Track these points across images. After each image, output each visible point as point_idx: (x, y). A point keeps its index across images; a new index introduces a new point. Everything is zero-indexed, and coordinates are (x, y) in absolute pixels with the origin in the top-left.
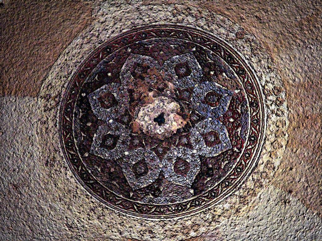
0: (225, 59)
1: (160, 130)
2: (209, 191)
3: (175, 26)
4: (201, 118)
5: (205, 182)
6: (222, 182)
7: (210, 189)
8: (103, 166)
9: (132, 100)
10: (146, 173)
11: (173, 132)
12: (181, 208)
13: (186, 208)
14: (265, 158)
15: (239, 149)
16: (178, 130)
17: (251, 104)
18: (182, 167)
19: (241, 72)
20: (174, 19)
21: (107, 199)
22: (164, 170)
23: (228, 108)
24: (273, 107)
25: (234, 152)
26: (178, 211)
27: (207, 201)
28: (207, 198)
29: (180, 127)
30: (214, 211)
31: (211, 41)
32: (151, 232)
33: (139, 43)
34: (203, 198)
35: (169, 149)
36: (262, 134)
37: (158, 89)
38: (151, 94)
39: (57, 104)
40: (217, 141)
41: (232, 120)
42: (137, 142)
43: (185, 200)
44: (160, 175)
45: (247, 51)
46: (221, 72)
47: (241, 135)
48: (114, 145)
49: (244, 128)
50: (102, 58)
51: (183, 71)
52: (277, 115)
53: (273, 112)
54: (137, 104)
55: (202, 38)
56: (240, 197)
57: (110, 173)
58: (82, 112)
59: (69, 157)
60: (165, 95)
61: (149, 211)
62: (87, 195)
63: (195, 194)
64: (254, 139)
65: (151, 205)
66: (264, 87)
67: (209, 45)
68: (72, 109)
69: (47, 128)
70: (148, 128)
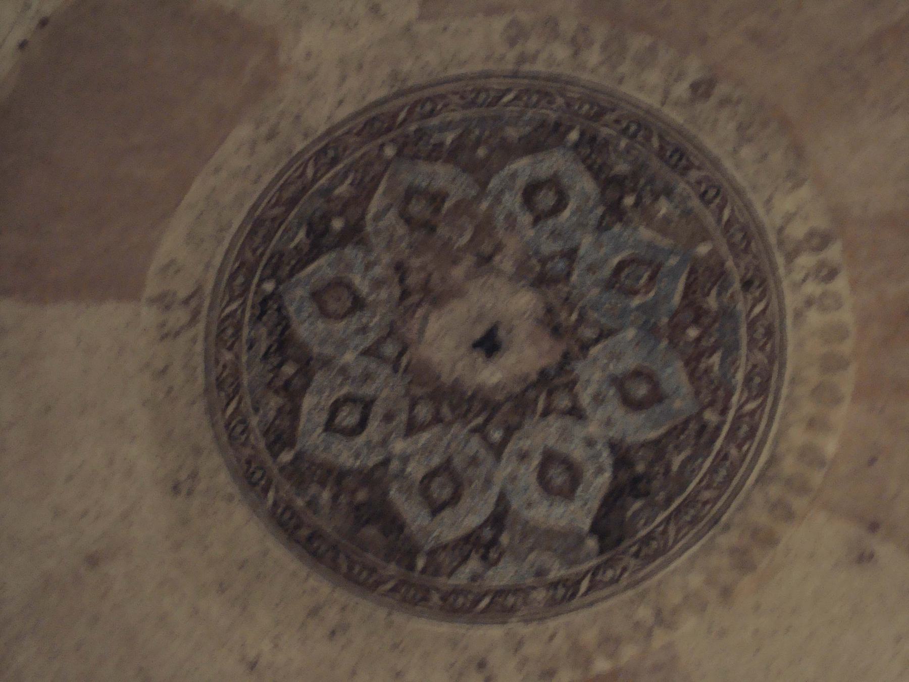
1: (491, 375)
3: (515, 75)
7: (643, 533)
10: (455, 499)
12: (565, 594)
14: (798, 436)
16: (543, 374)
17: (747, 285)
19: (715, 192)
20: (512, 55)
22: (510, 487)
24: (812, 288)
29: (544, 362)
36: (783, 366)
38: (458, 272)
40: (657, 397)
42: (423, 412)
45: (728, 129)
48: (362, 424)
49: (731, 350)
50: (315, 180)
51: (546, 199)
52: (824, 309)
53: (809, 302)
54: (419, 304)
56: (733, 551)
63: (602, 551)
64: (762, 384)
66: (781, 230)
68: (238, 329)
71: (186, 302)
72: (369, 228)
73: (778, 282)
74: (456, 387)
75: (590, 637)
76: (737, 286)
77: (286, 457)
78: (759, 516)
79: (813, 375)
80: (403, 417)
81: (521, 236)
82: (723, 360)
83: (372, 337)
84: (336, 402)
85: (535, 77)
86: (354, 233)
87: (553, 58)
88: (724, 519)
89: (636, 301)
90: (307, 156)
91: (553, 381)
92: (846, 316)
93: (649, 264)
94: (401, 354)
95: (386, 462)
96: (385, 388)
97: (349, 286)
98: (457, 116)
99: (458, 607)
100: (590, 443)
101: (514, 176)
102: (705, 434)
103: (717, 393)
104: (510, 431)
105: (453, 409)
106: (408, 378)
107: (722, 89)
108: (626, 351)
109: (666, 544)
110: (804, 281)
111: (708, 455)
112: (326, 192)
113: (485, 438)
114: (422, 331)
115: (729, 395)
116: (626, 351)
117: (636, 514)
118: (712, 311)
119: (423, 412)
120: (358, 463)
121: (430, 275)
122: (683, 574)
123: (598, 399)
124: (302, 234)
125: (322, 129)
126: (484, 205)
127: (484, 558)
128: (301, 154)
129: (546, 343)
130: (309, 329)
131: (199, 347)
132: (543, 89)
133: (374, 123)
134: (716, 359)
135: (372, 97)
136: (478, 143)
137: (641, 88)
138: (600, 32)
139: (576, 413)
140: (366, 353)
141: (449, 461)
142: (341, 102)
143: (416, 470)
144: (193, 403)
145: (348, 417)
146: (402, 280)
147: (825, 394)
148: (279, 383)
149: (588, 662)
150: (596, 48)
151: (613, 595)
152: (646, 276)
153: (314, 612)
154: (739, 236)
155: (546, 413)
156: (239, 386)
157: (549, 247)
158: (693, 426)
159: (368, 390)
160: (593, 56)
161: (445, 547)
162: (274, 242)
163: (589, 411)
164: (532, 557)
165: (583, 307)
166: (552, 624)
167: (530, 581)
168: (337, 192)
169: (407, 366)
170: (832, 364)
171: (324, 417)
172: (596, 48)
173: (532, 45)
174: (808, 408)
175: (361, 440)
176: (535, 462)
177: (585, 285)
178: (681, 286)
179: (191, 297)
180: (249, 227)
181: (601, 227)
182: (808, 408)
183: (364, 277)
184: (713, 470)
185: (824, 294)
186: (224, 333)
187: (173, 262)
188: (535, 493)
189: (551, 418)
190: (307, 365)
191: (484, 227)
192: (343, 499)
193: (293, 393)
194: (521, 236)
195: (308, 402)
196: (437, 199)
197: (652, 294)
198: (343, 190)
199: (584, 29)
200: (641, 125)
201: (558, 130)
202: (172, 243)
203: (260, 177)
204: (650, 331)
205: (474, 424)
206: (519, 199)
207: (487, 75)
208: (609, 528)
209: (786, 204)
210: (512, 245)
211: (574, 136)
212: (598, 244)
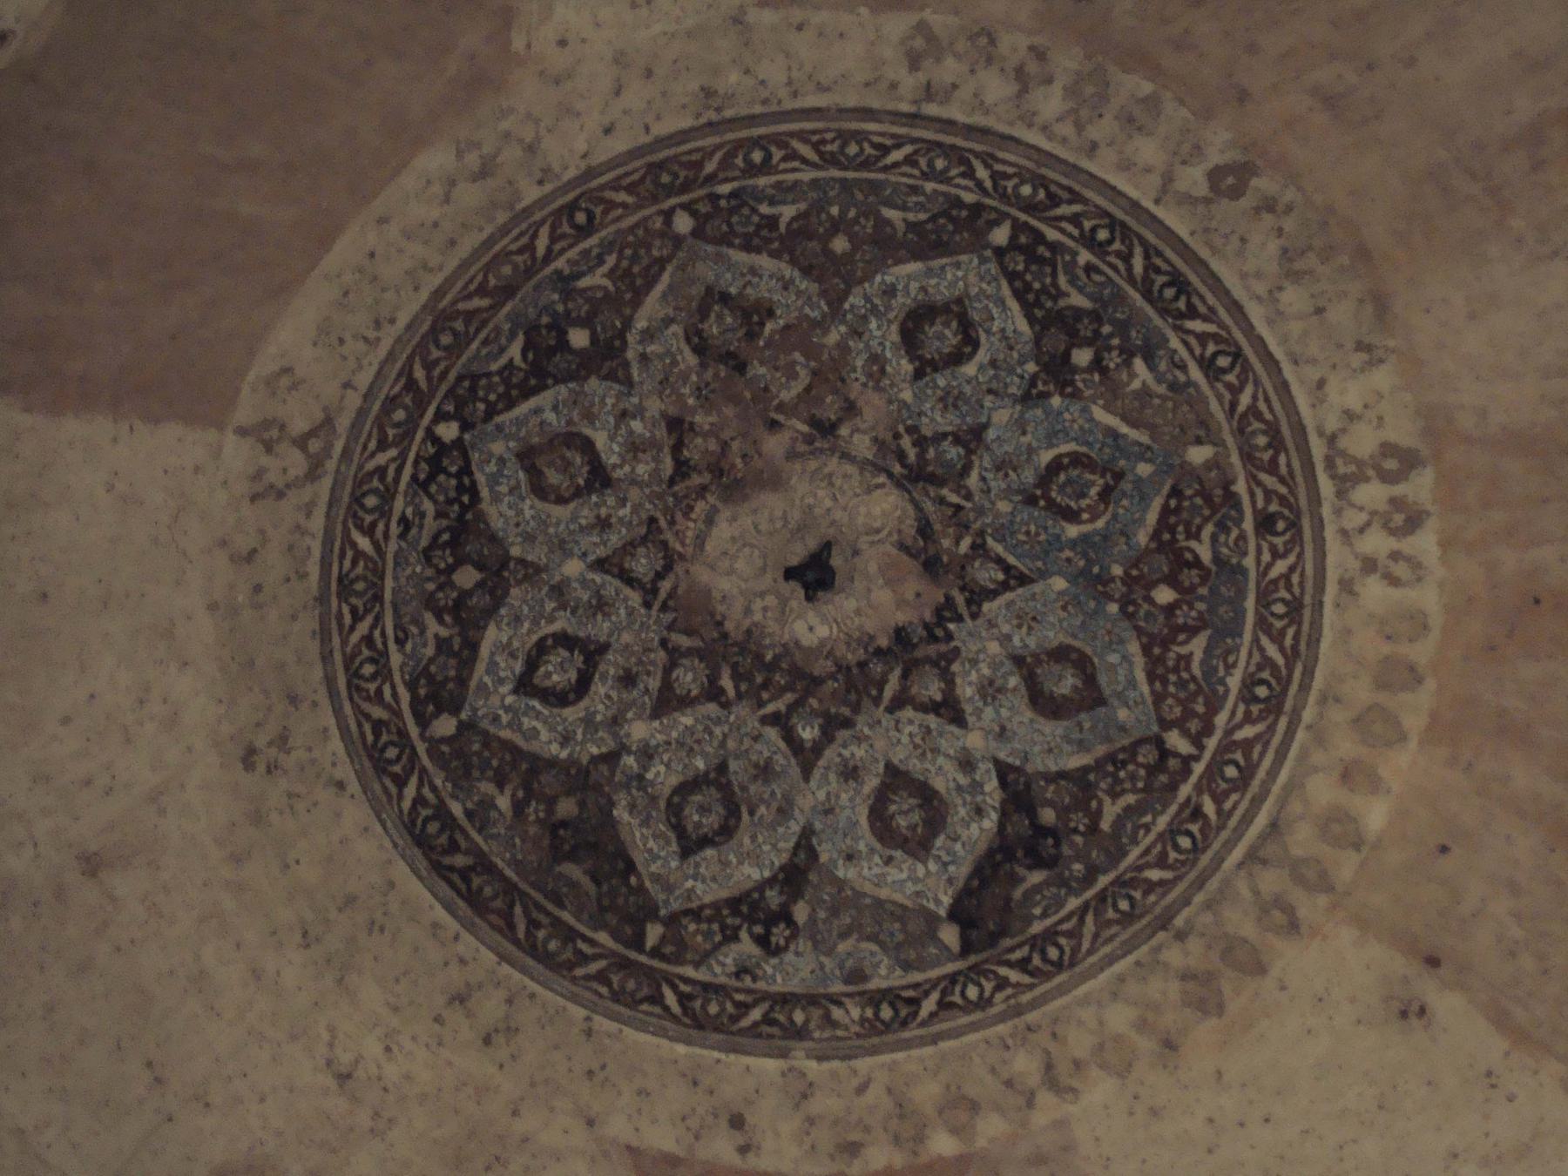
0: (1147, 295)
1: (812, 627)
2: (1034, 937)
3: (914, 118)
4: (1015, 579)
5: (1018, 893)
6: (1102, 897)
7: (1037, 928)
8: (527, 787)
9: (682, 468)
10: (727, 831)
11: (872, 638)
12: (893, 1016)
13: (916, 1014)
14: (1322, 791)
15: (1197, 742)
16: (900, 634)
17: (1265, 524)
18: (906, 813)
19: (1231, 357)
20: (910, 83)
21: (533, 950)
22: (818, 826)
23: (1156, 535)
24: (1376, 543)
25: (1164, 753)
26: (874, 1027)
27: (1018, 985)
28: (1025, 971)
29: (901, 618)
30: (1054, 1035)
31: (1084, 201)
32: (737, 1122)
33: (733, 195)
34: (1003, 971)
35: (847, 723)
36: (1309, 673)
37: (814, 422)
38: (775, 445)
39: (313, 474)
40: (1092, 697)
41: (1164, 595)
42: (688, 678)
43: (917, 977)
44: (797, 846)
45: (1265, 252)
46: (1128, 353)
47: (1209, 671)
48: (582, 686)
50: (549, 257)
52: (1393, 581)
53: (1369, 565)
54: (703, 490)
55: (1040, 182)
56: (1186, 976)
57: (555, 827)
58: (439, 515)
59: (362, 735)
60: (846, 456)
61: (734, 1019)
62: (436, 925)
63: (966, 948)
64: (1272, 697)
65: (749, 991)
66: (1332, 440)
67: (1075, 220)
68: (388, 496)
69: (258, 589)
70: (748, 611)
71: (301, 442)
72: (630, 355)
73: (1319, 525)
74: (749, 643)
75: (927, 1093)
76: (1248, 525)
77: (445, 726)
78: (1240, 922)
79: (1361, 692)
80: (654, 683)
81: (891, 396)
82: (1208, 651)
83: (615, 539)
84: (543, 640)
85: (948, 125)
86: (606, 357)
87: (980, 95)
88: (1179, 921)
89: (1073, 531)
90: (538, 216)
91: (917, 650)
92: (1428, 598)
93: (1104, 469)
94: (659, 576)
95: (611, 758)
96: (628, 628)
97: (588, 446)
98: (807, 175)
99: (707, 1017)
100: (966, 763)
101: (890, 291)
102: (1165, 769)
103: (1191, 701)
104: (832, 725)
105: (737, 677)
106: (668, 617)
107: (1263, 184)
108: (1045, 613)
109: (1075, 950)
110: (1362, 530)
111: (1165, 806)
112: (564, 282)
113: (790, 737)
114: (700, 540)
115: (1213, 708)
116: (1045, 613)
117: (1027, 895)
118: (1202, 562)
119: (688, 678)
120: (564, 754)
121: (725, 445)
122: (1099, 1004)
123: (990, 691)
124: (515, 351)
125: (571, 173)
126: (833, 337)
127: (763, 941)
128: (528, 211)
129: (914, 584)
130: (508, 511)
131: (317, 523)
132: (959, 147)
133: (662, 172)
134: (1197, 646)
135: (661, 129)
136: (836, 227)
137: (1125, 166)
138: (1067, 62)
139: (950, 710)
140: (600, 565)
141: (722, 768)
142: (608, 131)
143: (664, 777)
144: (294, 618)
145: (558, 671)
146: (677, 448)
147: (1377, 726)
148: (446, 598)
149: (920, 1139)
150: (1057, 89)
151: (974, 1027)
152: (1093, 491)
153: (459, 999)
154: (1262, 440)
155: (898, 703)
156: (378, 598)
157: (937, 420)
158: (1147, 755)
159: (600, 629)
160: (1050, 103)
161: (695, 914)
162: (464, 359)
163: (968, 709)
164: (842, 947)
165: (981, 533)
166: (863, 1064)
167: (837, 988)
168: (584, 283)
169: (670, 596)
170: (1397, 675)
171: (518, 667)
172: (1057, 89)
173: (949, 70)
174: (1346, 746)
175: (572, 713)
176: (871, 783)
177: (991, 493)
178: (1152, 517)
179: (312, 433)
180: (425, 327)
181: (1029, 398)
182: (1346, 746)
183: (612, 438)
184: (1172, 832)
185: (1395, 556)
186: (361, 502)
187: (287, 370)
188: (865, 839)
189: (908, 713)
190: (499, 572)
191: (830, 374)
192: (534, 810)
193: (468, 619)
194: (891, 396)
195: (492, 635)
196: (754, 314)
197: (1100, 524)
198: (596, 279)
199: (1040, 54)
200: (1120, 229)
201: (974, 220)
202: (292, 335)
203: (453, 243)
204: (1093, 582)
205: (770, 708)
206: (894, 335)
207: (867, 113)
208: (981, 913)
209: (1348, 393)
210: (873, 407)
211: (1000, 236)
212: (1021, 426)
